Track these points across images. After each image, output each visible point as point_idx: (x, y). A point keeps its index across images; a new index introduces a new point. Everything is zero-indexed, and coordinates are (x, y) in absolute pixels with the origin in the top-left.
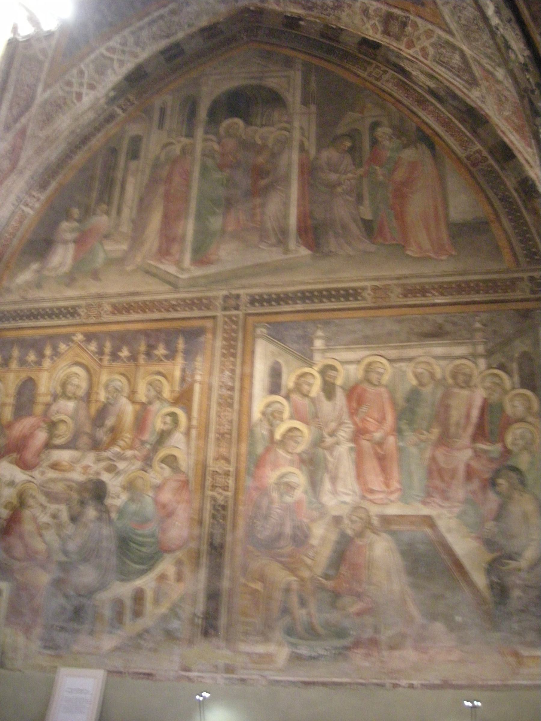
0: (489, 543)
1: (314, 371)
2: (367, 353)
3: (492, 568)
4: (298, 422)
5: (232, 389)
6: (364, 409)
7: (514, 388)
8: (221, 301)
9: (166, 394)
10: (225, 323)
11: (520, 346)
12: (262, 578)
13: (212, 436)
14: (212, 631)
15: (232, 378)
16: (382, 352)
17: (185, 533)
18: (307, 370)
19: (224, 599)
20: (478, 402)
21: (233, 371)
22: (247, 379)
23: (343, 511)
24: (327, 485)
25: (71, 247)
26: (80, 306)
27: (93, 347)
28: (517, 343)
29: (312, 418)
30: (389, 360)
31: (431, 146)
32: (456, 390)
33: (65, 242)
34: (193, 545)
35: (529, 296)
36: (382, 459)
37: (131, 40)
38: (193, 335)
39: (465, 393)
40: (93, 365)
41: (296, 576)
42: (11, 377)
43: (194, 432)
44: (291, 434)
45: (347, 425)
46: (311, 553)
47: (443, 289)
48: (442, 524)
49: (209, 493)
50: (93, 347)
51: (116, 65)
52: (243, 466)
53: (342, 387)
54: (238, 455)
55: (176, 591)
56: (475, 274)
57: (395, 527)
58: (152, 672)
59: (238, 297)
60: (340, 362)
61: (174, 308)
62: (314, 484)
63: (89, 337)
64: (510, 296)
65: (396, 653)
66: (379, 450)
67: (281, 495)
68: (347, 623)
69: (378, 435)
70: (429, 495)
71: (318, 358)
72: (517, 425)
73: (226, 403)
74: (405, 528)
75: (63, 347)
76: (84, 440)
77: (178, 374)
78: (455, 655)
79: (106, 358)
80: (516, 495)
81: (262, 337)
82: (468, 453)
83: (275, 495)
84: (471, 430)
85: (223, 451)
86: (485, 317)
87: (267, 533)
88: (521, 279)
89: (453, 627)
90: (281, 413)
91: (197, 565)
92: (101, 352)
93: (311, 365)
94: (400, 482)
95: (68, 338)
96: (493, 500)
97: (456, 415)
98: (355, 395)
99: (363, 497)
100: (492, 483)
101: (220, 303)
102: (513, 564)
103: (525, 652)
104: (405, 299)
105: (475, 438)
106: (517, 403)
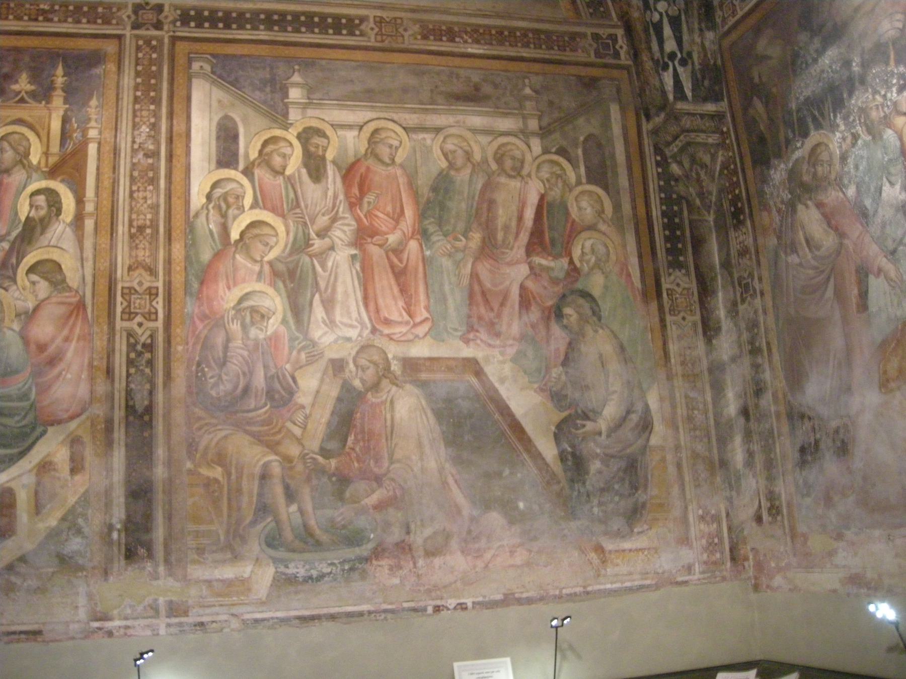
0: (557, 397)
1: (291, 135)
2: (373, 115)
3: (561, 432)
4: (271, 214)
5: (155, 154)
6: (370, 198)
7: (579, 183)
8: (129, 11)
9: (35, 158)
10: (138, 48)
11: (585, 127)
12: (221, 459)
14: (142, 551)
16: (395, 117)
17: (83, 390)
18: (278, 132)
19: (159, 497)
20: (533, 199)
21: (154, 127)
22: (178, 142)
23: (347, 352)
24: (319, 312)
28: (581, 121)
29: (291, 207)
30: (404, 128)
32: (503, 180)
34: (99, 410)
35: (593, 58)
36: (400, 274)
38: (82, 64)
39: (515, 184)
41: (276, 454)
43: (89, 224)
44: (256, 231)
45: (346, 222)
46: (300, 417)
47: (478, 34)
48: (490, 371)
49: (119, 324)
52: (178, 280)
53: (334, 162)
54: (169, 261)
55: (73, 489)
56: (523, 19)
57: (424, 376)
58: (42, 627)
60: (332, 125)
62: (298, 311)
64: (568, 56)
65: (437, 561)
66: (395, 260)
67: (244, 327)
68: (362, 522)
69: (393, 239)
70: (471, 328)
71: (294, 115)
72: (584, 235)
73: (144, 177)
74: (438, 376)
77: (56, 125)
78: (520, 557)
80: (589, 330)
81: (204, 76)
82: (523, 270)
83: (235, 327)
84: (524, 238)
85: (143, 254)
86: (537, 80)
87: (226, 387)
88: (583, 35)
89: (513, 517)
90: (239, 197)
91: (109, 444)
93: (286, 127)
94: (427, 308)
96: (559, 337)
97: (503, 215)
98: (355, 177)
99: (374, 331)
100: (557, 313)
101: (129, 17)
102: (590, 426)
103: (609, 546)
104: (424, 42)
105: (530, 250)
106: (584, 204)
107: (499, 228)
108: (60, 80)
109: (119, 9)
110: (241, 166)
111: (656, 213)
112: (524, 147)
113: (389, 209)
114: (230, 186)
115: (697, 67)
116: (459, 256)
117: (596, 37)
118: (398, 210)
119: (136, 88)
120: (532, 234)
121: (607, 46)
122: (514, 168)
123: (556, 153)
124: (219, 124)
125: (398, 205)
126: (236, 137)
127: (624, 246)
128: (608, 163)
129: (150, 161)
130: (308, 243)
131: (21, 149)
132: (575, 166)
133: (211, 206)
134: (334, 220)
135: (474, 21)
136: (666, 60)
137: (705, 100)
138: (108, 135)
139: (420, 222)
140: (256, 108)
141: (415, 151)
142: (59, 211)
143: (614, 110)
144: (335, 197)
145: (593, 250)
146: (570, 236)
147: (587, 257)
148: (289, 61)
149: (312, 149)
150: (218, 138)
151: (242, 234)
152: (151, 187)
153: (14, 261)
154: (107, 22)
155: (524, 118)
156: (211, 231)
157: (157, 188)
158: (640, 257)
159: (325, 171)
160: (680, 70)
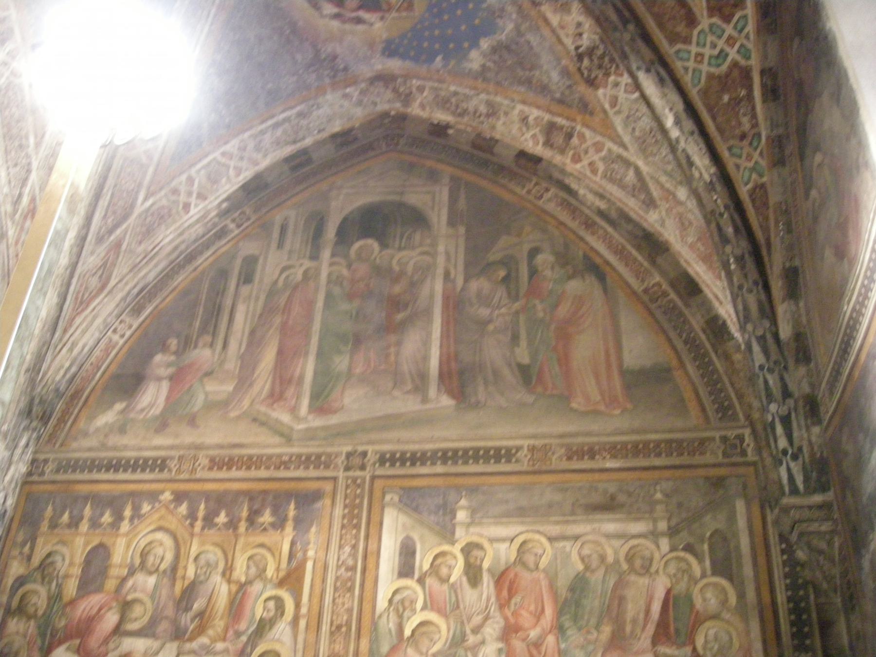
1: (456, 549)
5: (353, 569)
6: (517, 599)
7: (704, 575)
8: (343, 457)
9: (270, 572)
10: (347, 487)
11: (712, 523)
13: (325, 628)
15: (354, 555)
16: (541, 529)
18: (446, 548)
20: (660, 594)
21: (354, 547)
22: (370, 558)
25: (165, 386)
26: (172, 458)
27: (183, 509)
28: (708, 518)
29: (451, 609)
31: (601, 277)
32: (633, 578)
33: (159, 379)
35: (720, 459)
37: (251, 145)
38: (307, 500)
39: (644, 581)
40: (182, 533)
42: (79, 541)
43: (302, 623)
44: (424, 629)
47: (614, 451)
50: (183, 509)
51: (232, 172)
56: (656, 432)
59: (364, 454)
61: (286, 465)
63: (179, 497)
64: (697, 459)
69: (533, 634)
71: (459, 532)
72: (708, 624)
73: (344, 586)
75: (146, 508)
76: (163, 627)
77: (286, 548)
79: (199, 524)
81: (392, 504)
84: (651, 629)
86: (667, 486)
88: (713, 439)
90: (413, 602)
92: (192, 516)
93: (453, 543)
95: (153, 497)
97: (632, 610)
98: (506, 582)
106: (709, 595)
107: (628, 620)
108: (292, 512)
109: (336, 457)
110: (416, 576)
111: (781, 597)
112: (653, 547)
113: (532, 608)
114: (406, 593)
115: (807, 460)
116: (591, 648)
117: (724, 439)
118: (540, 608)
119: (344, 517)
120: (658, 625)
121: (734, 446)
122: (643, 566)
123: (685, 549)
124: (402, 542)
125: (540, 604)
126: (414, 553)
127: (748, 633)
128: (733, 555)
129: (349, 574)
130: (463, 638)
131: (261, 567)
132: (701, 560)
133: (392, 609)
134: (487, 618)
135: (613, 439)
136: (780, 455)
137: (814, 491)
138: (322, 554)
139: (558, 619)
140: (431, 529)
141: (556, 559)
142: (282, 614)
143: (740, 506)
144: (488, 600)
145: (716, 638)
146: (694, 626)
147: (709, 646)
148: (458, 488)
149: (472, 560)
150: (400, 554)
151: (413, 632)
152: (348, 595)
153: (249, 650)
154: (327, 467)
155: (655, 521)
156: (390, 630)
157: (353, 595)
158: (764, 642)
159: (481, 577)
160: (792, 465)
